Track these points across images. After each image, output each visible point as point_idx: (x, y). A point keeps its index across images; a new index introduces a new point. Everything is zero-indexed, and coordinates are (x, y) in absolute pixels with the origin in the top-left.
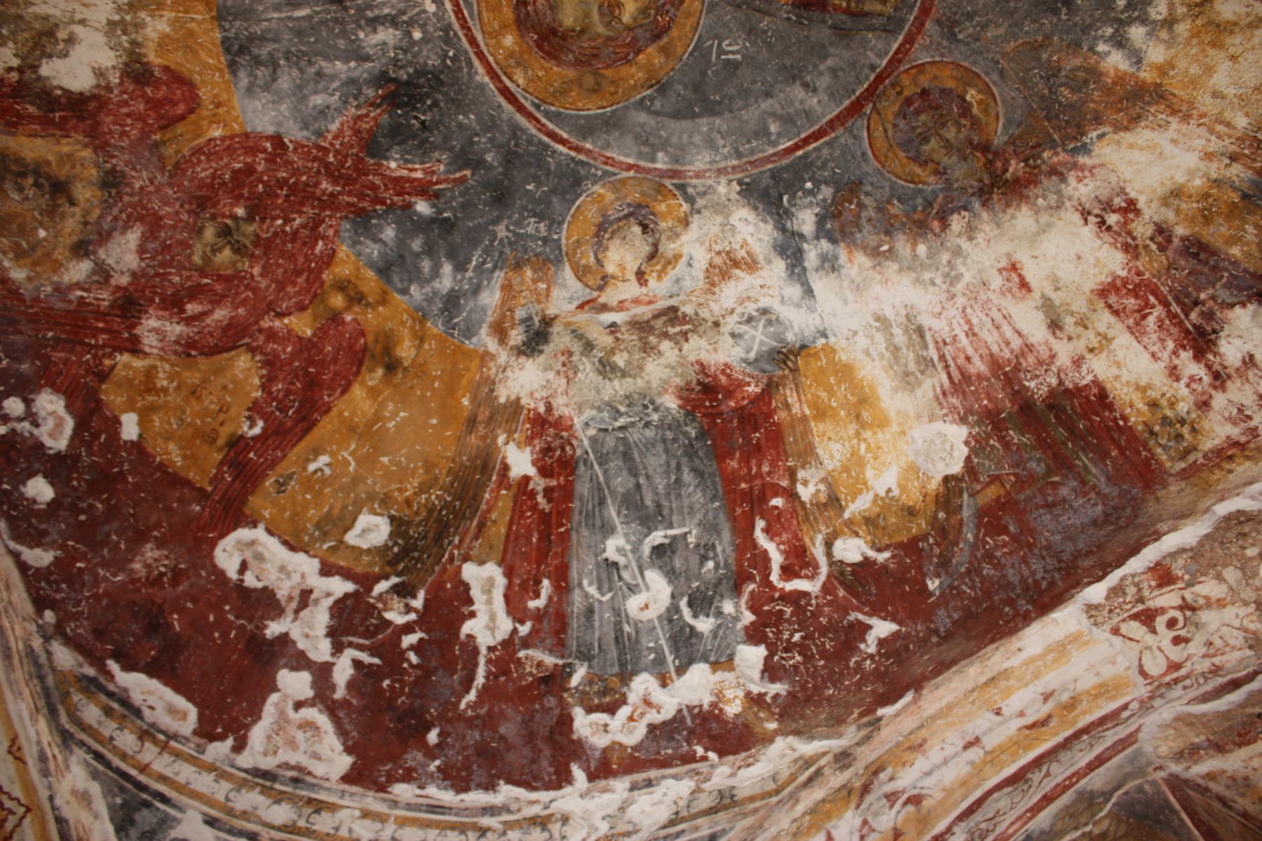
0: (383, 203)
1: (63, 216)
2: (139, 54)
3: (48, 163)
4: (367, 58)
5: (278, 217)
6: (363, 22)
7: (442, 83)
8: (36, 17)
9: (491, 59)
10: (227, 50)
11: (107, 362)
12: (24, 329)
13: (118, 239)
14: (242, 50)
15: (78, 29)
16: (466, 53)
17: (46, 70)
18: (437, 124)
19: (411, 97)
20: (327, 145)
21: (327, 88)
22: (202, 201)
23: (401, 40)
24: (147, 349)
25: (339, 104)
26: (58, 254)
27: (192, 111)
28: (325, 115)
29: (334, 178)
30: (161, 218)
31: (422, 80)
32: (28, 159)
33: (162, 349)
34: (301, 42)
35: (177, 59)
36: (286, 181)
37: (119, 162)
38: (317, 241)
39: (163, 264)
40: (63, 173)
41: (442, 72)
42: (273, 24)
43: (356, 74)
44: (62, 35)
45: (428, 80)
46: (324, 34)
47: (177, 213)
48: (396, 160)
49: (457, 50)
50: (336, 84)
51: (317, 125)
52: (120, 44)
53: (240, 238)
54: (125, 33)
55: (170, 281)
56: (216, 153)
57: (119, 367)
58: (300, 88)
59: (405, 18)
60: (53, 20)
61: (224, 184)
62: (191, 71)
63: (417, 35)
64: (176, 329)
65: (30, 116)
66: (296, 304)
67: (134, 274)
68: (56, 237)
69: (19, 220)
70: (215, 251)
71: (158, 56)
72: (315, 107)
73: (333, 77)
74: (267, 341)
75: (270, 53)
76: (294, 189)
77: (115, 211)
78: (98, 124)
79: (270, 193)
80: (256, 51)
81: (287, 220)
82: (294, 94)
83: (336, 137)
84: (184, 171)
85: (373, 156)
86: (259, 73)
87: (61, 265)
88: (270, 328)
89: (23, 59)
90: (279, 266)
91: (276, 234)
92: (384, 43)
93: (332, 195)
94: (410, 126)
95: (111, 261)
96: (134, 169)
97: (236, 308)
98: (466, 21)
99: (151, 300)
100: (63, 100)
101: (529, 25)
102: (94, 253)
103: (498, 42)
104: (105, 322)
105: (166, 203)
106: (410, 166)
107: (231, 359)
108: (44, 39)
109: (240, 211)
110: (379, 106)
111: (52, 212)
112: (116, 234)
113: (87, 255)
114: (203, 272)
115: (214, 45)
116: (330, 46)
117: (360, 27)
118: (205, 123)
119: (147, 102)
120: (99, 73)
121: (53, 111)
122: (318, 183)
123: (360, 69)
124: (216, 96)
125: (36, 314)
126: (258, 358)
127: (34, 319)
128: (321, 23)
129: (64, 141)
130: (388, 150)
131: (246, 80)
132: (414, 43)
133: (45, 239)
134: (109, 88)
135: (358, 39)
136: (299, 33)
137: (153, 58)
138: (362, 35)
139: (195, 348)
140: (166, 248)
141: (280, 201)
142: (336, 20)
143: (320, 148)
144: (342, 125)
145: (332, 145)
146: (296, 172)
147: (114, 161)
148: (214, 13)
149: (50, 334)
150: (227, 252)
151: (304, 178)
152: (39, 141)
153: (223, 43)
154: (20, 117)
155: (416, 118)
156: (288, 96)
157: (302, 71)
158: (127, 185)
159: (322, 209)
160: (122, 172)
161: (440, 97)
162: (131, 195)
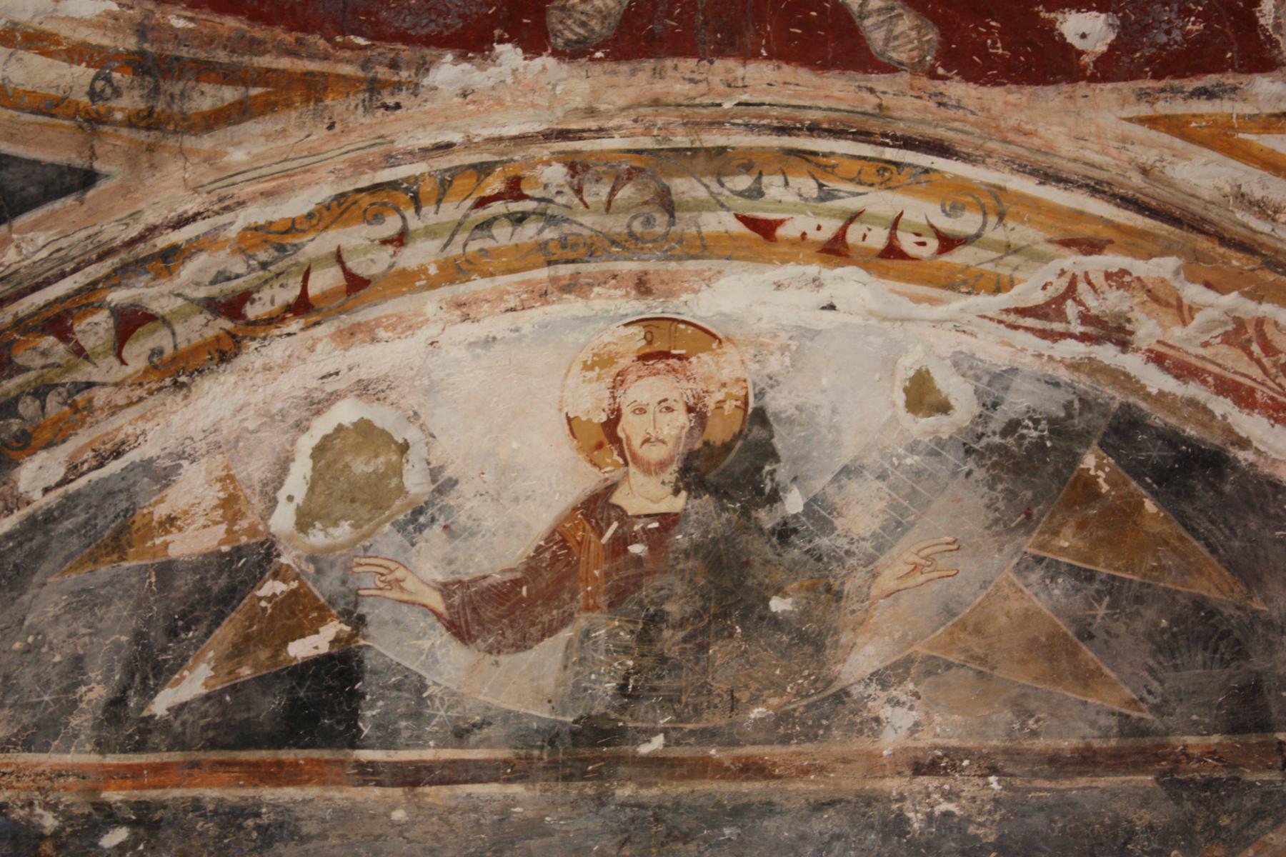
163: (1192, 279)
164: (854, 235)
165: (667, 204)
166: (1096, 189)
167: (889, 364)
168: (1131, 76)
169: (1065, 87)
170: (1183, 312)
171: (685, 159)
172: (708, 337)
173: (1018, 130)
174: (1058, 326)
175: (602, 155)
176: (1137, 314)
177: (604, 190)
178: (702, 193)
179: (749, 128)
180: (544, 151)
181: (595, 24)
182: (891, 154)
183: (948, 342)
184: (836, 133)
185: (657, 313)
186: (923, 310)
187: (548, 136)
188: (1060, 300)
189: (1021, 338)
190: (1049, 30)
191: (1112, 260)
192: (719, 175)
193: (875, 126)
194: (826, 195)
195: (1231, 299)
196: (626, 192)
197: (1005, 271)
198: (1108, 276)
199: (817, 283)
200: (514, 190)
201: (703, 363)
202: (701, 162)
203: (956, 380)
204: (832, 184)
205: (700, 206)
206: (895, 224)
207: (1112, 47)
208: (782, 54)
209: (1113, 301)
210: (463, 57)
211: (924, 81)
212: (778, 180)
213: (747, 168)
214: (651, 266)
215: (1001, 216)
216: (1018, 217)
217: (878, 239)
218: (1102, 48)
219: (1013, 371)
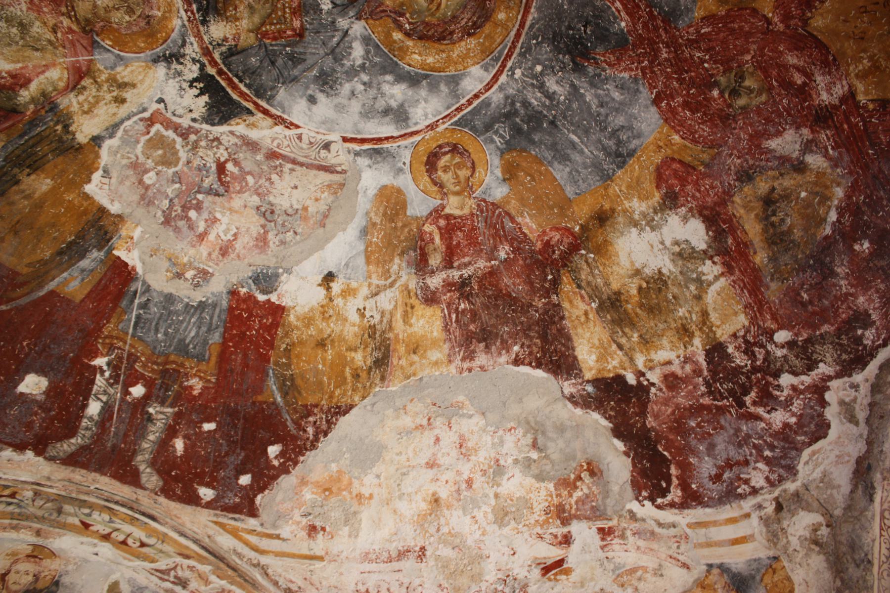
0: (651, 12)
1: (785, 189)
2: (660, 206)
3: (757, 215)
4: (573, 85)
5: (704, 68)
6: (555, 103)
7: (555, 33)
8: (676, 265)
9: (520, 17)
10: (624, 162)
11: (871, 107)
12: (876, 169)
13: (780, 151)
14: (618, 155)
15: (668, 243)
16: (527, 33)
17: (703, 246)
18: (580, 18)
19: (576, 44)
20: (639, 71)
21: (606, 95)
22: (724, 119)
23: (548, 75)
24: (846, 88)
25: (610, 82)
26: (812, 178)
27: (673, 159)
28: (622, 85)
29: (656, 52)
30: (751, 136)
31: (562, 46)
32: (762, 226)
33: (840, 79)
34: (591, 128)
35: (648, 184)
36: (678, 80)
37: (731, 179)
38: (703, 34)
39: (780, 115)
40: (758, 205)
41: (548, 39)
42: (592, 148)
43: (586, 85)
44: (677, 249)
45: (559, 43)
46: (577, 118)
47: (741, 128)
48: (619, 25)
49: (530, 40)
50: (600, 92)
51: (632, 85)
52: (661, 218)
53: (733, 81)
54: (653, 220)
55: (789, 105)
56: (688, 131)
57: (870, 97)
58: (617, 110)
59: (535, 82)
60: (672, 257)
61: (705, 114)
62: (650, 174)
63: (539, 68)
64: (820, 80)
65: (734, 239)
66: (753, 17)
67: (798, 128)
68: (801, 186)
69: (803, 211)
70: (750, 90)
71: (654, 196)
72: (622, 94)
73: (597, 96)
74: (793, 17)
75: (610, 139)
76: (680, 71)
77: (763, 163)
78: (715, 204)
79: (692, 83)
80: (614, 148)
81: (702, 61)
82: (623, 110)
83: (632, 70)
84: (712, 141)
85: (627, 40)
86: (625, 137)
87: (818, 173)
88: (781, 22)
89: (704, 260)
90: (735, 46)
91: (715, 62)
92: (557, 82)
93: (668, 47)
94: (593, 32)
95: (797, 147)
96: (729, 169)
97: (781, 52)
98: (510, 48)
99: (809, 107)
100: (714, 228)
101: (484, 12)
102: (798, 159)
103: (507, 21)
104: (842, 125)
105: (740, 139)
106: (617, 13)
107: (820, 31)
108: (685, 256)
109: (715, 93)
110: (594, 59)
111: (786, 196)
112: (777, 155)
113: (802, 162)
114: (770, 88)
115: (626, 171)
116: (582, 111)
117: (558, 102)
118: (674, 148)
119: (685, 186)
120: (685, 219)
121: (724, 230)
122: (666, 60)
123: (581, 85)
124: (654, 152)
125: (861, 168)
126: (809, 15)
127: (866, 167)
128: (572, 124)
129: (738, 215)
130: (617, 34)
131: (634, 142)
132: (545, 67)
133: (806, 191)
134: (691, 210)
135: (566, 99)
136: (587, 132)
137: (657, 197)
138: (562, 98)
139: (827, 59)
140: (768, 120)
141: (693, 74)
142: (565, 117)
143: (644, 74)
144: (621, 71)
145: (637, 69)
146: (668, 77)
147: (732, 182)
148: (609, 182)
149: (870, 152)
150: (747, 83)
151: (669, 70)
152: (747, 227)
153: (622, 168)
154: (738, 244)
155: (585, 31)
156: (626, 113)
157: (607, 115)
158: (742, 167)
159: (681, 45)
160: (736, 174)
161: (563, 28)
162: (747, 161)
163: (214, 573)
164: (114, 535)
165: (60, 511)
166: (196, 541)
167: (107, 576)
168: (214, 509)
169: (194, 507)
170: (207, 582)
171: (72, 500)
172: (53, 554)
173: (176, 516)
174: (166, 577)
175: (46, 493)
176: (193, 580)
177: (42, 503)
178: (72, 511)
179: (97, 497)
180: (29, 487)
181: (61, 454)
182: (137, 516)
183: (129, 574)
184: (123, 505)
185: (40, 543)
186: (126, 562)
187: (33, 483)
188: (170, 570)
189: (154, 578)
190: (195, 491)
191: (191, 563)
192: (80, 507)
193: (135, 506)
194: (111, 521)
195: (224, 582)
196: (49, 505)
197: (157, 557)
198: (188, 567)
199: (95, 545)
200: (13, 495)
201: (47, 562)
202: (77, 502)
203: (127, 586)
204: (114, 519)
205: (70, 514)
206: (129, 535)
207: (212, 500)
208: (115, 476)
209: (187, 574)
210: (15, 451)
211: (153, 495)
212: (98, 513)
213: (90, 507)
214: (44, 527)
215: (163, 542)
216: (168, 543)
217: (121, 538)
218: (209, 499)
219: (146, 588)
